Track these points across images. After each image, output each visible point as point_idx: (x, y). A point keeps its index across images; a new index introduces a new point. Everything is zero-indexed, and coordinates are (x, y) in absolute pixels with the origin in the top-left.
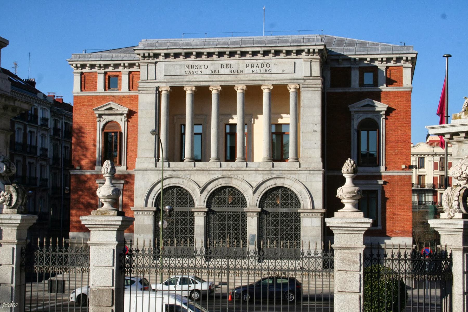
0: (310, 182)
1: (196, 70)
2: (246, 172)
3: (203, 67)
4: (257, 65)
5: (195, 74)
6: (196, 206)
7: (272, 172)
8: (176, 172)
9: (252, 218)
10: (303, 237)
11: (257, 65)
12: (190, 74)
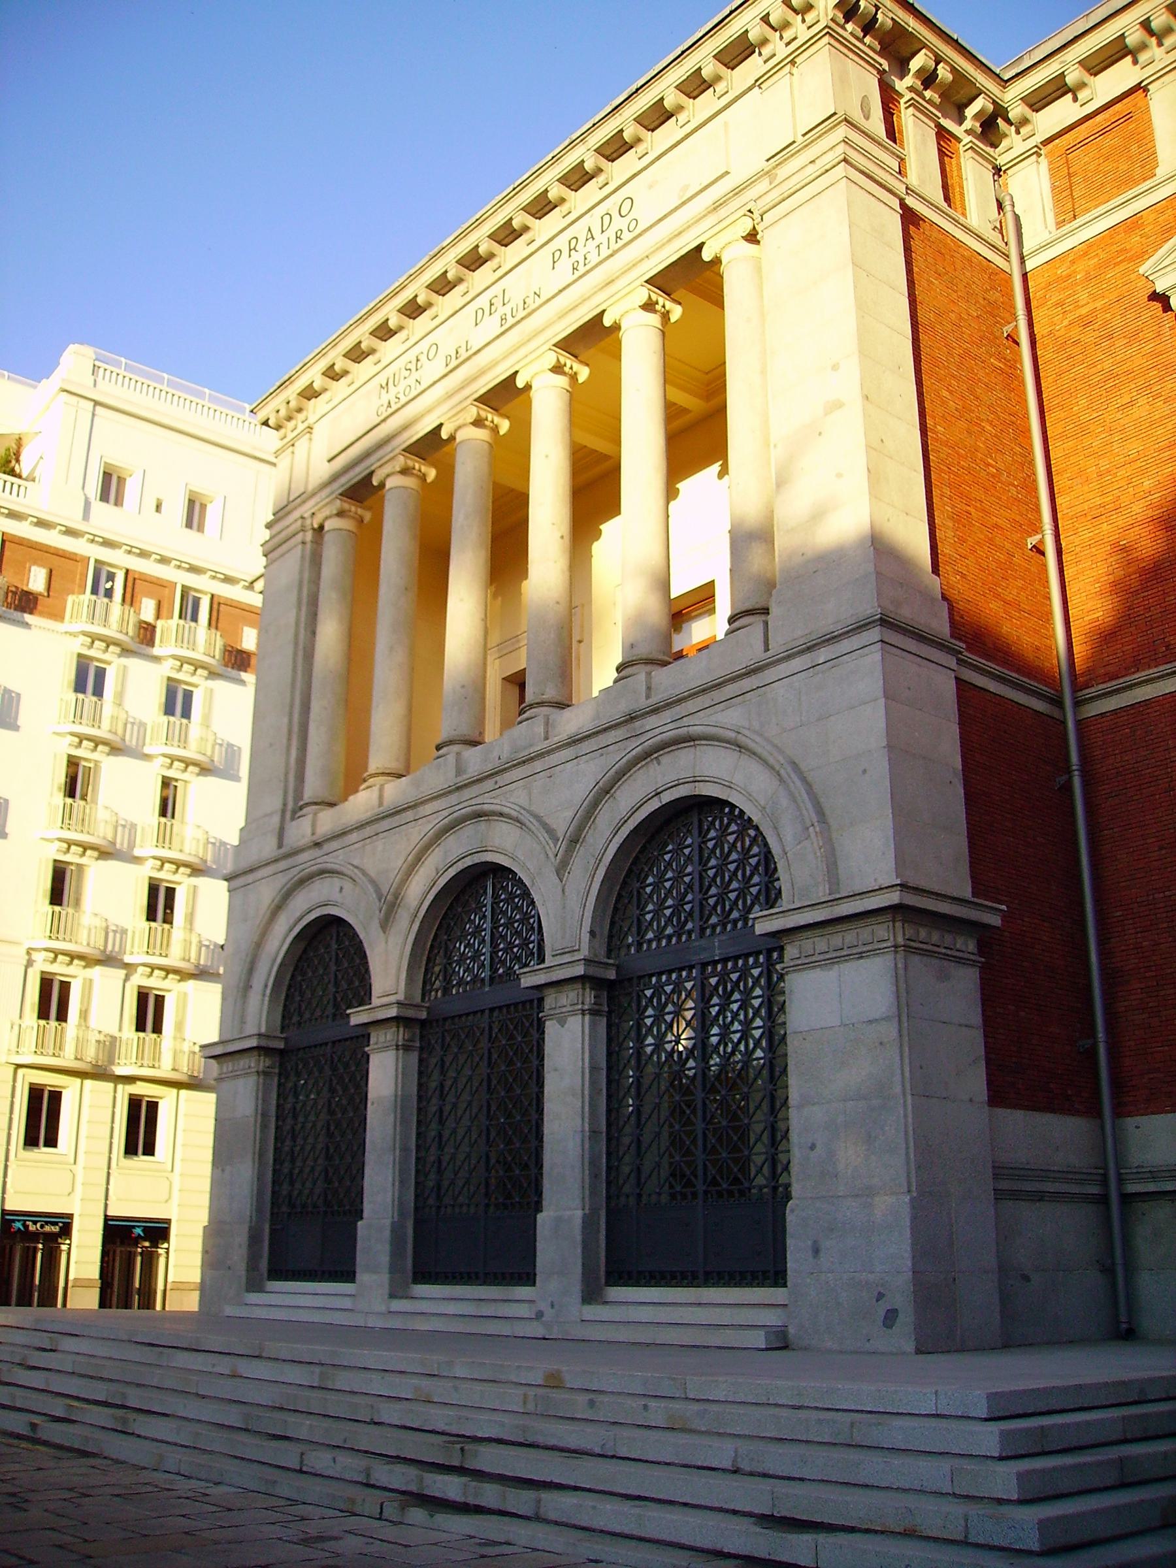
0: (818, 720)
1: (408, 382)
2: (538, 765)
3: (423, 358)
4: (589, 230)
5: (404, 400)
6: (376, 1001)
7: (638, 724)
8: (327, 847)
9: (562, 1022)
10: (800, 1107)
11: (589, 230)
12: (390, 411)
